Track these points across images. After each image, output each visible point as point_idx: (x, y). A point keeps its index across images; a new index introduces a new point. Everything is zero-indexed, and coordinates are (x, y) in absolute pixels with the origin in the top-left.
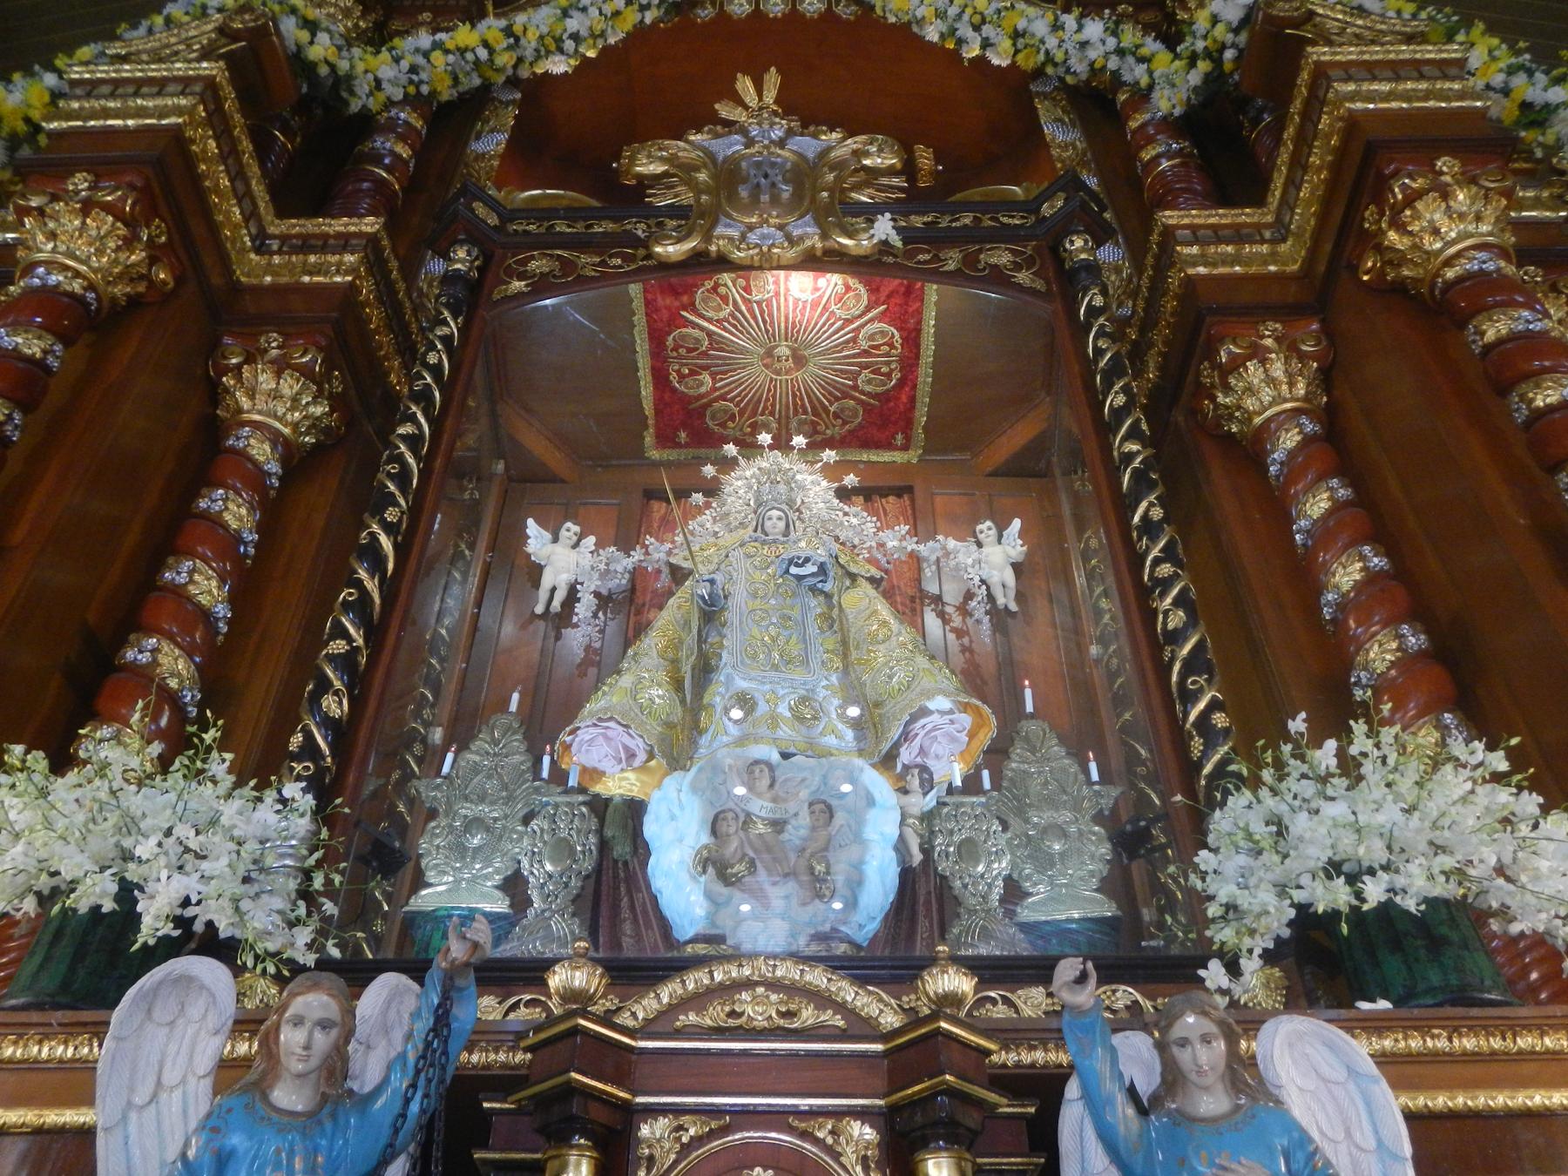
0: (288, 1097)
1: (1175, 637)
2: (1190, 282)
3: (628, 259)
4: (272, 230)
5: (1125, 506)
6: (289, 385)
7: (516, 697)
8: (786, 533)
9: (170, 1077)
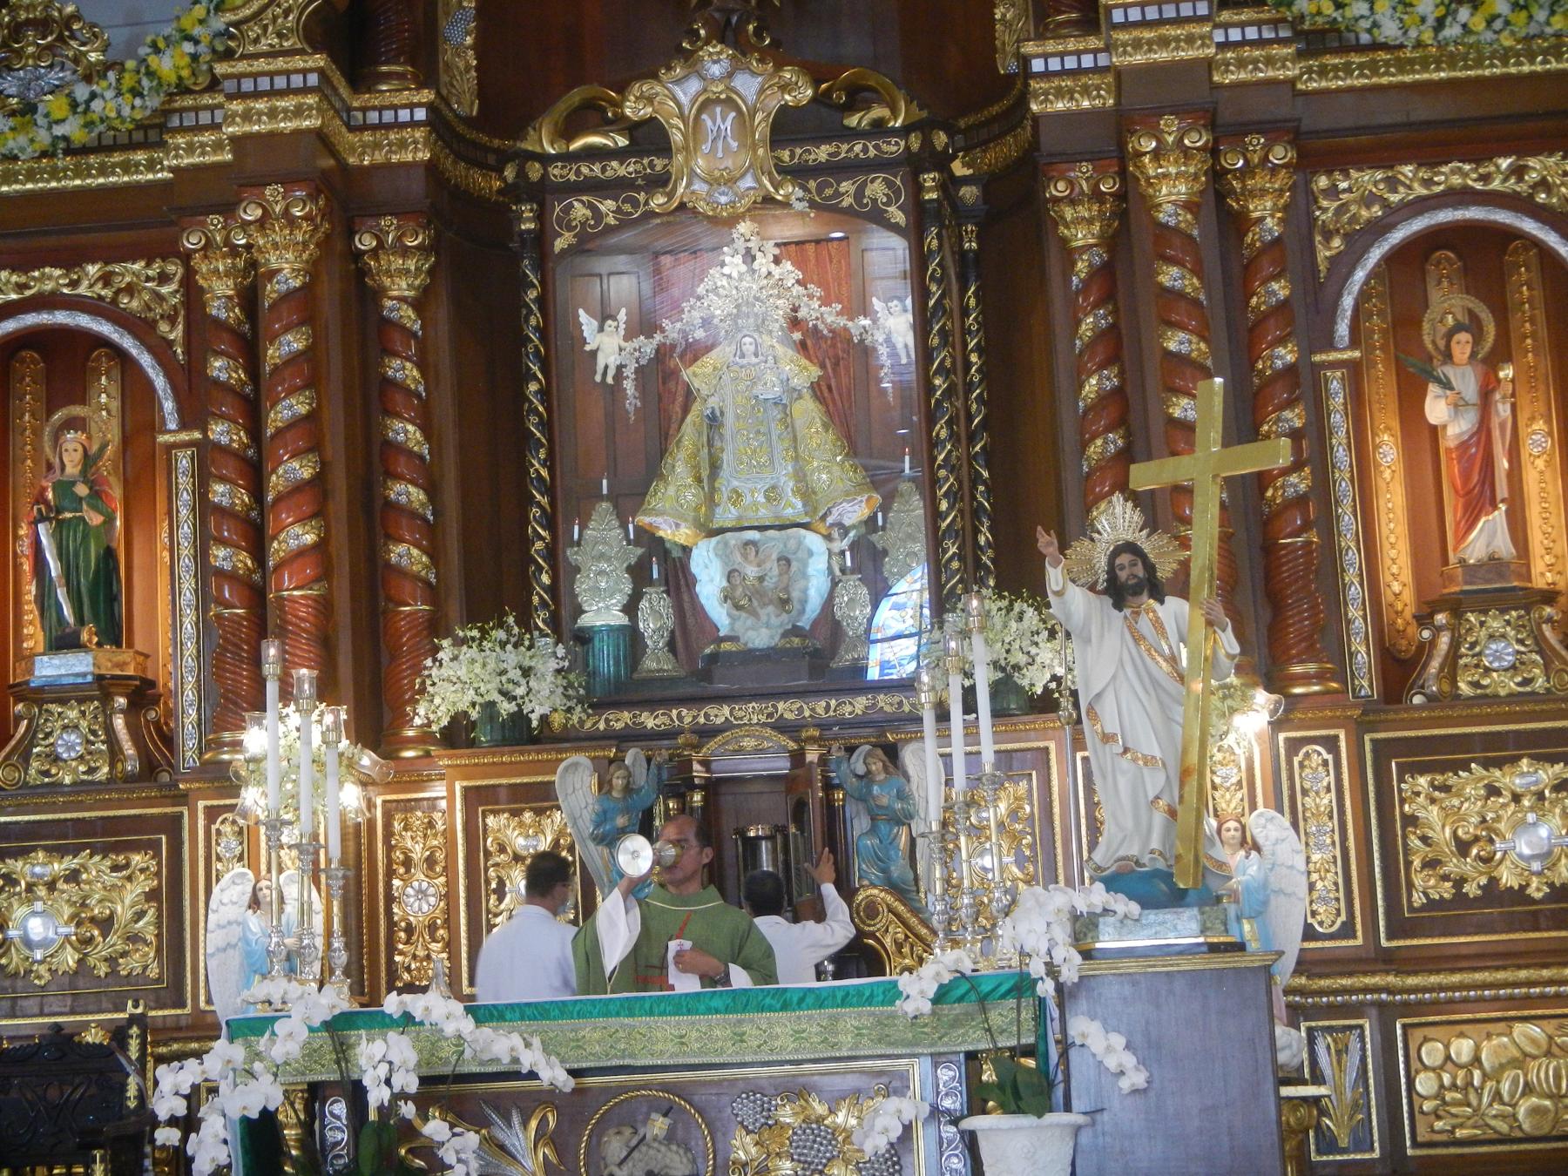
0: (615, 794)
1: (943, 516)
2: (1036, 119)
3: (635, 203)
4: (355, 104)
5: (931, 420)
6: (411, 264)
7: (605, 482)
9: (578, 786)
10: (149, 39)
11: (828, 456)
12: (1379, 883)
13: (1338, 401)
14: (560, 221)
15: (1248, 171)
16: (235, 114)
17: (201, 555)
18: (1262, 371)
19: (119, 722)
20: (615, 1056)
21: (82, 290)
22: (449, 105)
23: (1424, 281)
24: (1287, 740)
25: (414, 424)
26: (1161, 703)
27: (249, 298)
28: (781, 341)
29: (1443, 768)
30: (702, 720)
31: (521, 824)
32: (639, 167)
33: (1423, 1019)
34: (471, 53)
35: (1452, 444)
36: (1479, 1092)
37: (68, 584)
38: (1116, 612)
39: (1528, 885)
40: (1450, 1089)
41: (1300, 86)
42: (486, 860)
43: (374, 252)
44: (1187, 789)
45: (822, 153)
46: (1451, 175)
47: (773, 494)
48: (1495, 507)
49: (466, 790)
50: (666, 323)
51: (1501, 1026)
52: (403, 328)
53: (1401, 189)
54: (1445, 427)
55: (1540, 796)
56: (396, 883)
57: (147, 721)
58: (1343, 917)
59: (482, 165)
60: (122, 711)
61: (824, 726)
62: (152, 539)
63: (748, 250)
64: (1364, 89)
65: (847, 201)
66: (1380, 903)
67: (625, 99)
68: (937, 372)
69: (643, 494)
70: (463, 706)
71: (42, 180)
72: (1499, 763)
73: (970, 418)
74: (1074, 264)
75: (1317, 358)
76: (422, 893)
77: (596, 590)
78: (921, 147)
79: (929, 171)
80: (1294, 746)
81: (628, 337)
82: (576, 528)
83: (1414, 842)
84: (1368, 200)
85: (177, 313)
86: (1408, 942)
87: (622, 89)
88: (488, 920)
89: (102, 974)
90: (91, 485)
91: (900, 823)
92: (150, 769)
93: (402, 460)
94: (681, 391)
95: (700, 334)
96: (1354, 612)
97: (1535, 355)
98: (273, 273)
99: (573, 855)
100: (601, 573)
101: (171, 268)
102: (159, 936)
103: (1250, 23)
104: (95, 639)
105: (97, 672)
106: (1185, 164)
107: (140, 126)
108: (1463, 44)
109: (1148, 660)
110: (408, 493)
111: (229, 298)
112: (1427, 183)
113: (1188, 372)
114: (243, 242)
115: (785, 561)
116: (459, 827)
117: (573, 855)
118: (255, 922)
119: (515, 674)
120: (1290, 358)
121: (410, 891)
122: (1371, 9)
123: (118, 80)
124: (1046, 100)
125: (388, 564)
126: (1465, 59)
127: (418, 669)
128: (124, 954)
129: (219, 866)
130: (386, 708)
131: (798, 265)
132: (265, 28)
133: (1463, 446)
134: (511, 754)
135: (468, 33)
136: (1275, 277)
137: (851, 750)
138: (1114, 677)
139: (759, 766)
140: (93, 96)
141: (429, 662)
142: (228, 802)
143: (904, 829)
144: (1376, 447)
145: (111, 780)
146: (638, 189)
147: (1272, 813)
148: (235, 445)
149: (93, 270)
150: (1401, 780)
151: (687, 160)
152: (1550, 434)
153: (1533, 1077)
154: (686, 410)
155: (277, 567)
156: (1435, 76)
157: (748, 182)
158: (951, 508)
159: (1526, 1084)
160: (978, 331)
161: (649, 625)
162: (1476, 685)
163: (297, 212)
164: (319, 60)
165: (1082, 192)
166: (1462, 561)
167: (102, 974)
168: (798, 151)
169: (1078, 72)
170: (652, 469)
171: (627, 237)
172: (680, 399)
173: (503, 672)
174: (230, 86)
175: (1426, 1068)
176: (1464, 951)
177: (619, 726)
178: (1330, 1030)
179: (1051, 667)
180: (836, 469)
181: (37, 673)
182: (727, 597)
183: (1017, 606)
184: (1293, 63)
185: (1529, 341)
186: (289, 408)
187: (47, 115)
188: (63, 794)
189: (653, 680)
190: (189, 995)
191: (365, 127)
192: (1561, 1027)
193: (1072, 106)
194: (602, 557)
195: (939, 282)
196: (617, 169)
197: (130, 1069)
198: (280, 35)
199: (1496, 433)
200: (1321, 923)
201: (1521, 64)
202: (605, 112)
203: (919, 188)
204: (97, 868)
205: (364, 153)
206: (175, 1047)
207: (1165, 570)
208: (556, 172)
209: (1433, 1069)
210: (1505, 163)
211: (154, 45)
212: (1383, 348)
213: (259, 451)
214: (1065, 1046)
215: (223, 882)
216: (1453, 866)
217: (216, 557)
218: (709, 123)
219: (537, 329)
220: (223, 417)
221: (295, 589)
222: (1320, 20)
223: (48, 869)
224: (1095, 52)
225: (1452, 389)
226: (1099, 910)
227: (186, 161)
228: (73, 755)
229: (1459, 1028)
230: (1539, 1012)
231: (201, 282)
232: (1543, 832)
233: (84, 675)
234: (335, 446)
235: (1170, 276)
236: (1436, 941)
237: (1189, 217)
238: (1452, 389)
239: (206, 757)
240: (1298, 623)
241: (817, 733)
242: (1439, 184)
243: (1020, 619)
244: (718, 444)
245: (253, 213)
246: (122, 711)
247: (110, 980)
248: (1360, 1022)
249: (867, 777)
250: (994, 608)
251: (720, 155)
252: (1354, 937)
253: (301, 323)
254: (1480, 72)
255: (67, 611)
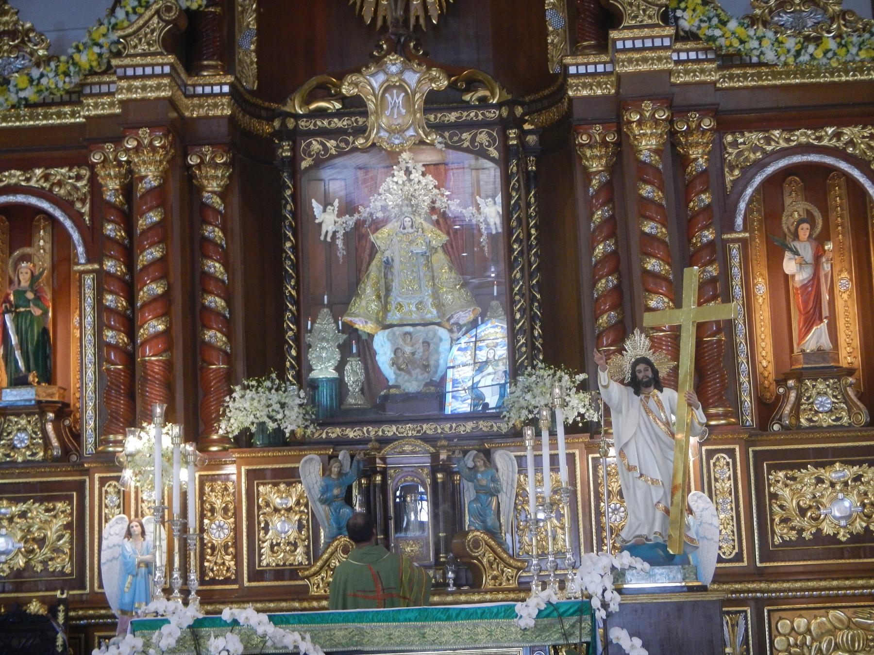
0: (333, 476)
1: (518, 322)
2: (571, 100)
4: (189, 83)
7: (326, 297)
8: (412, 226)
9: (312, 471)
10: (74, 44)
11: (451, 285)
12: (756, 531)
13: (736, 261)
14: (304, 151)
15: (689, 132)
16: (122, 88)
17: (99, 333)
18: (695, 244)
19: (49, 427)
20: (352, 645)
21: (33, 183)
22: (241, 83)
23: (782, 194)
24: (707, 450)
25: (219, 263)
26: (661, 449)
27: (128, 190)
28: (425, 220)
29: (791, 467)
30: (380, 433)
31: (279, 491)
32: (349, 122)
33: (780, 607)
34: (253, 54)
35: (798, 285)
36: (810, 648)
37: (21, 349)
38: (635, 397)
39: (838, 533)
40: (793, 647)
41: (718, 85)
42: (259, 511)
43: (198, 166)
44: (675, 497)
45: (452, 117)
46: (801, 136)
47: (420, 305)
48: (821, 321)
49: (248, 472)
50: (361, 208)
51: (823, 611)
52: (214, 209)
53: (773, 143)
54: (793, 276)
55: (846, 484)
56: (206, 521)
57: (64, 426)
58: (736, 550)
59: (259, 117)
60: (51, 421)
61: (449, 438)
62: (68, 322)
63: (407, 168)
64: (754, 87)
65: (466, 144)
66: (756, 542)
67: (342, 84)
68: (515, 241)
69: (347, 303)
70: (247, 424)
71: (11, 121)
72: (823, 465)
73: (530, 265)
74: (591, 181)
75: (725, 236)
76: (220, 527)
77: (319, 358)
78: (508, 115)
79: (512, 129)
80: (710, 454)
81: (340, 215)
82: (309, 323)
83: (776, 508)
84: (755, 149)
85: (86, 198)
86: (772, 564)
87: (341, 77)
88: (259, 545)
89: (39, 570)
90: (35, 292)
91: (492, 495)
92: (66, 452)
93: (212, 283)
94: (368, 246)
95: (380, 215)
96: (743, 379)
97: (843, 236)
98: (142, 178)
99: (308, 509)
100: (323, 348)
101: (83, 172)
102: (71, 549)
103: (692, 50)
104: (36, 380)
105: (38, 399)
106: (655, 128)
107: (68, 92)
108: (810, 65)
109: (654, 423)
110: (215, 302)
111: (117, 190)
112: (788, 140)
113: (656, 244)
114: (125, 159)
115: (426, 343)
116: (244, 492)
117: (308, 509)
118: (128, 545)
119: (277, 407)
120: (711, 237)
121: (213, 526)
122: (760, 44)
123: (57, 67)
124: (577, 89)
125: (203, 341)
126: (810, 73)
127: (220, 402)
128: (52, 559)
129: (107, 511)
130: (200, 421)
131: (436, 177)
132: (140, 40)
133: (804, 287)
134: (273, 451)
135: (252, 43)
136: (704, 191)
137: (465, 453)
138: (635, 434)
139: (414, 461)
140: (42, 76)
141: (227, 399)
142: (112, 475)
143: (495, 498)
144: (755, 285)
145: (44, 460)
146: (349, 135)
147: (701, 493)
148: (119, 273)
149: (38, 172)
150: (769, 474)
151: (377, 119)
152: (851, 280)
153: (839, 640)
154: (372, 256)
155: (143, 344)
156: (793, 81)
157: (411, 132)
158: (522, 317)
159: (836, 644)
160: (535, 216)
161: (350, 379)
162: (810, 420)
163: (157, 144)
164: (171, 58)
165: (596, 142)
166: (803, 351)
167: (39, 570)
168: (439, 115)
169: (595, 74)
170: (353, 289)
171: (339, 161)
172: (368, 251)
173: (269, 406)
174: (120, 72)
175: (780, 634)
176: (801, 569)
177: (333, 436)
178: (728, 613)
179: (578, 408)
180: (456, 293)
181: (3, 399)
182: (394, 363)
183: (559, 373)
184: (716, 73)
185: (840, 228)
186: (152, 253)
187: (16, 86)
188: (18, 468)
189: (352, 410)
190: (88, 583)
191: (195, 95)
192: (855, 613)
193: (592, 93)
194: (323, 339)
195: (518, 190)
196: (337, 123)
197: (59, 629)
198: (149, 44)
199: (823, 280)
200: (724, 553)
201: (841, 76)
202: (329, 90)
203: (506, 138)
204: (37, 512)
205: (193, 110)
206: (80, 613)
207: (663, 372)
208: (303, 124)
209: (785, 635)
210: (830, 130)
211: (77, 48)
212: (759, 230)
213: (132, 277)
214: (607, 643)
215: (111, 523)
216: (797, 522)
217: (107, 336)
218: (389, 99)
219: (291, 212)
220: (111, 257)
221: (152, 356)
222: (731, 50)
223: (9, 510)
224: (605, 63)
225: (799, 255)
226: (627, 567)
227: (93, 113)
228: (23, 445)
229: (799, 612)
230: (844, 604)
231: (100, 181)
232: (847, 504)
233: (30, 400)
234: (176, 273)
235: (646, 191)
236: (787, 564)
237: (657, 157)
238: (799, 255)
239: (100, 448)
240: (713, 385)
241: (446, 443)
242: (794, 141)
243: (560, 381)
244: (390, 277)
245: (131, 144)
246: (51, 421)
247: (43, 573)
248: (745, 608)
249: (474, 469)
250: (546, 374)
251: (395, 117)
252: (743, 561)
253: (158, 206)
254: (818, 80)
255: (21, 364)
